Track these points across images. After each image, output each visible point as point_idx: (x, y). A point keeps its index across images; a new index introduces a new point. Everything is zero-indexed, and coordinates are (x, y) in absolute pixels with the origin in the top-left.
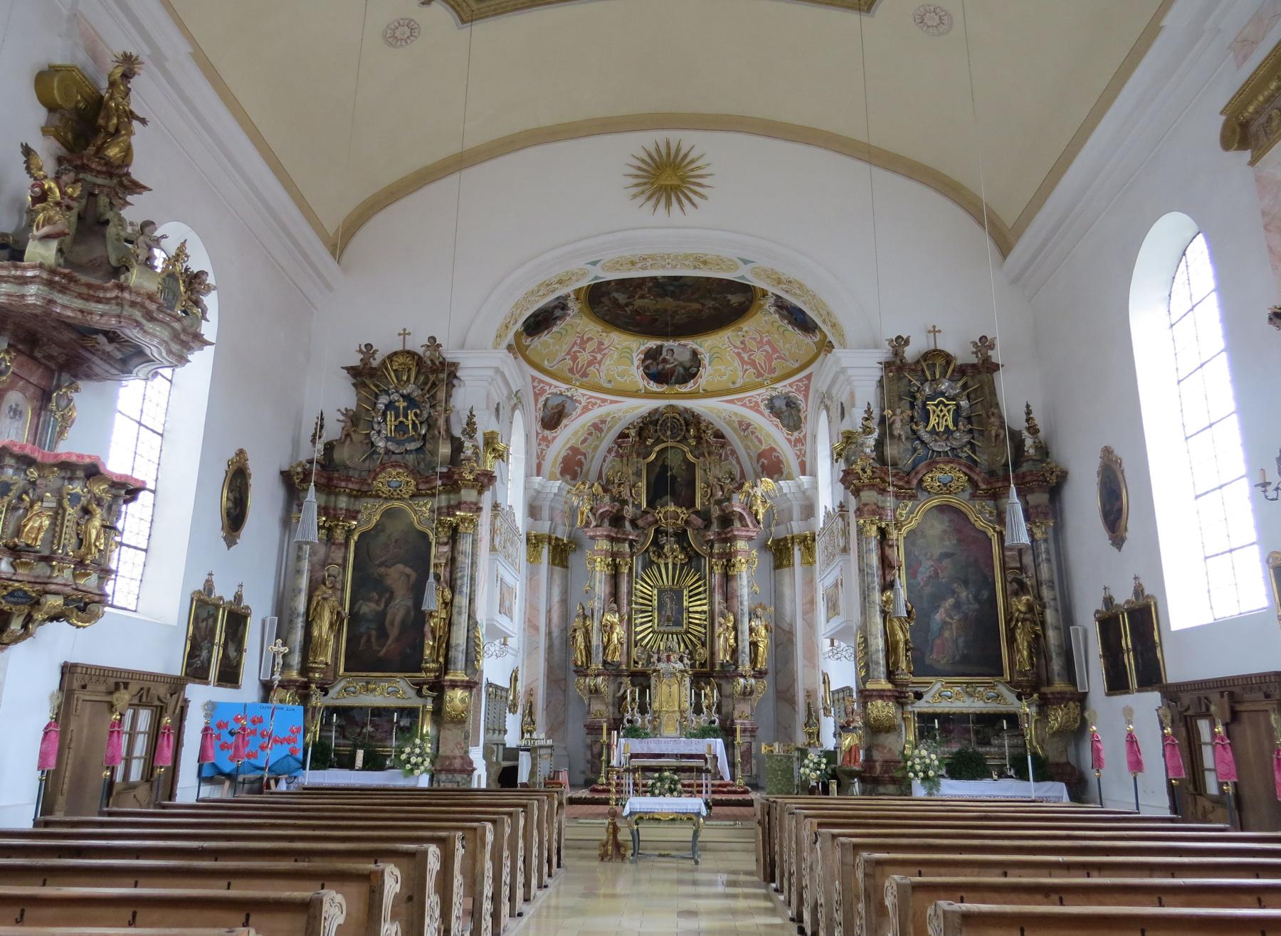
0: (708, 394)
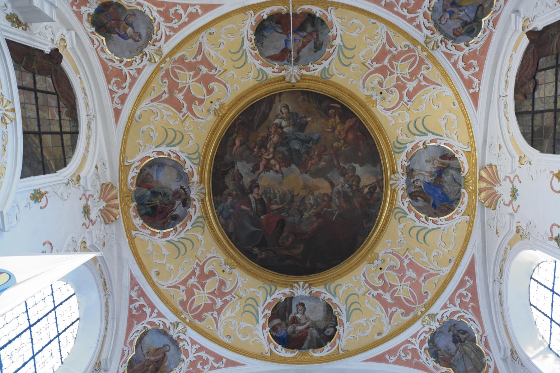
0: (349, 354)
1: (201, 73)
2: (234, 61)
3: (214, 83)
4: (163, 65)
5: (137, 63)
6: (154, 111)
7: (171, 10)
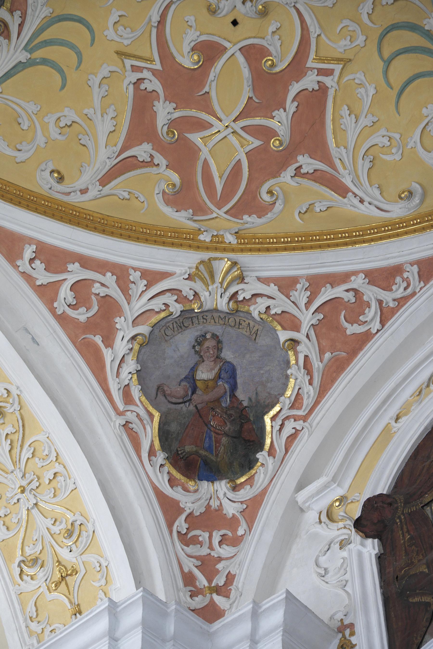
1: (177, 114)
2: (79, 54)
3: (179, 59)
4: (230, 239)
5: (269, 302)
6: (367, 165)
7: (83, 318)
